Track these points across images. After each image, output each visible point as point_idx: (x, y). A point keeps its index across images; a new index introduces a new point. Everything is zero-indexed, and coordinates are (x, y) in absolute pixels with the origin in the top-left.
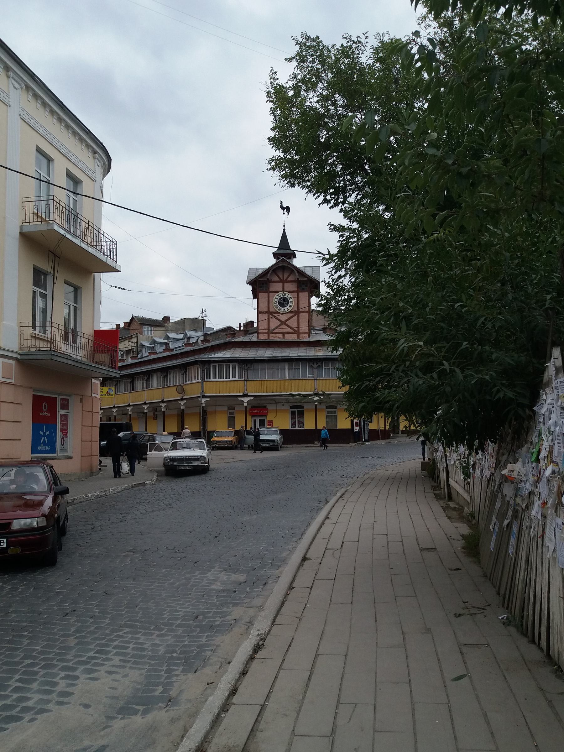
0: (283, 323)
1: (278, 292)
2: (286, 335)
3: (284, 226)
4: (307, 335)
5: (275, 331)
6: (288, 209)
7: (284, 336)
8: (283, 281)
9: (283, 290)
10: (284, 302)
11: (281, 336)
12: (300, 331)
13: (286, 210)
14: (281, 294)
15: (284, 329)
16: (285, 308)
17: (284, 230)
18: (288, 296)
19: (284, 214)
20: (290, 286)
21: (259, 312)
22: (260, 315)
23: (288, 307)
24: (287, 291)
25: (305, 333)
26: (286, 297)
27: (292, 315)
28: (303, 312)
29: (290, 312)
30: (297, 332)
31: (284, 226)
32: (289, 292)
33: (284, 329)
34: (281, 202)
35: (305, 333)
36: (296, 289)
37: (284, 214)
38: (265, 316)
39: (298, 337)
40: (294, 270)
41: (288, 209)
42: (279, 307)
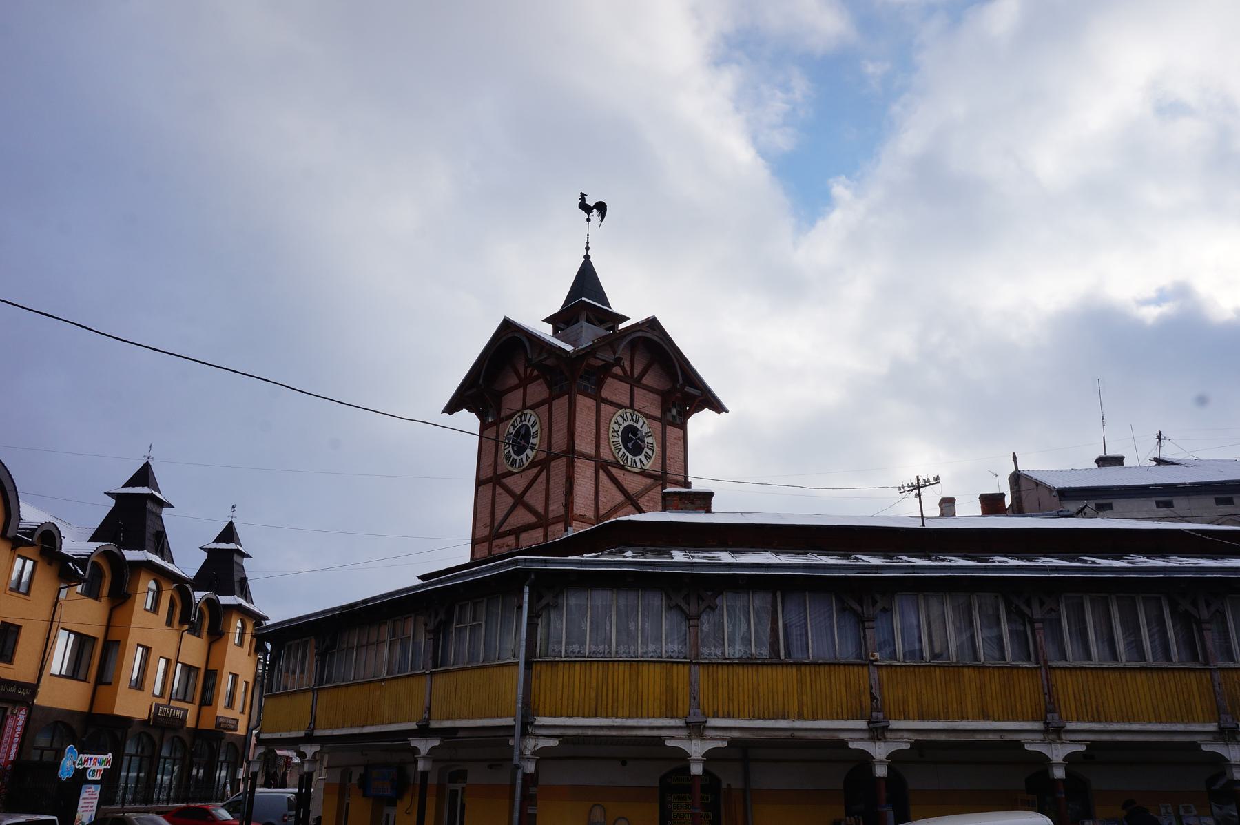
0: (519, 500)
1: (510, 417)
2: (523, 536)
3: (587, 248)
4: (561, 526)
5: (503, 529)
6: (601, 207)
7: (517, 539)
8: (524, 383)
9: (524, 407)
10: (523, 437)
11: (511, 540)
12: (551, 515)
13: (595, 211)
14: (519, 419)
15: (522, 517)
16: (523, 456)
17: (587, 257)
18: (532, 419)
19: (589, 220)
20: (538, 391)
21: (480, 483)
22: (480, 489)
23: (528, 451)
24: (527, 409)
25: (557, 520)
26: (526, 423)
27: (535, 470)
28: (557, 456)
29: (533, 464)
30: (543, 522)
31: (587, 248)
32: (532, 408)
33: (522, 517)
34: (583, 196)
35: (557, 520)
36: (545, 394)
37: (589, 220)
38: (487, 490)
39: (546, 536)
40: (524, 339)
41: (601, 207)
42: (513, 456)
